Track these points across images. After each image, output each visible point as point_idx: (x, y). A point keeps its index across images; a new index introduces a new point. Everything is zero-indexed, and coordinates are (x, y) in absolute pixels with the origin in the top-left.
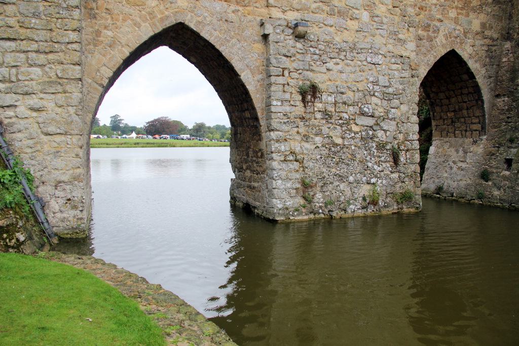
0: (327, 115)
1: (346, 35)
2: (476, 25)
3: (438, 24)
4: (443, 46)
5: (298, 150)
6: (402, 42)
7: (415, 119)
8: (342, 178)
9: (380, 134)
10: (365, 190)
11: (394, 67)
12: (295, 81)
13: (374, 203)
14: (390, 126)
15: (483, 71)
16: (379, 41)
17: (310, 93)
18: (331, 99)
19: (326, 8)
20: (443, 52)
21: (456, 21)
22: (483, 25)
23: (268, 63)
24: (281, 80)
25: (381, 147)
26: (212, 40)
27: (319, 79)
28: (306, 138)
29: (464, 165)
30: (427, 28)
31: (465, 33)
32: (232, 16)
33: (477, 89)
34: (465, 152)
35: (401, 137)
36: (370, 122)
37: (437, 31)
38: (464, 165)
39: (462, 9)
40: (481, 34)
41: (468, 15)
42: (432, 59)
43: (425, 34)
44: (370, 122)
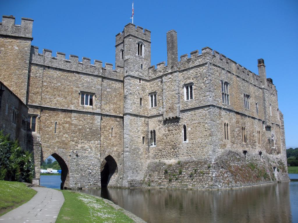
1: (85, 154)
2: (115, 149)
3: (106, 150)
4: (107, 154)
6: (97, 155)
11: (95, 160)
19: (82, 149)
20: (107, 155)
21: (110, 149)
22: (117, 149)
26: (60, 156)
30: (103, 151)
31: (112, 151)
32: (64, 151)
34: (115, 177)
37: (106, 151)
40: (116, 151)
41: (113, 147)
42: (105, 157)
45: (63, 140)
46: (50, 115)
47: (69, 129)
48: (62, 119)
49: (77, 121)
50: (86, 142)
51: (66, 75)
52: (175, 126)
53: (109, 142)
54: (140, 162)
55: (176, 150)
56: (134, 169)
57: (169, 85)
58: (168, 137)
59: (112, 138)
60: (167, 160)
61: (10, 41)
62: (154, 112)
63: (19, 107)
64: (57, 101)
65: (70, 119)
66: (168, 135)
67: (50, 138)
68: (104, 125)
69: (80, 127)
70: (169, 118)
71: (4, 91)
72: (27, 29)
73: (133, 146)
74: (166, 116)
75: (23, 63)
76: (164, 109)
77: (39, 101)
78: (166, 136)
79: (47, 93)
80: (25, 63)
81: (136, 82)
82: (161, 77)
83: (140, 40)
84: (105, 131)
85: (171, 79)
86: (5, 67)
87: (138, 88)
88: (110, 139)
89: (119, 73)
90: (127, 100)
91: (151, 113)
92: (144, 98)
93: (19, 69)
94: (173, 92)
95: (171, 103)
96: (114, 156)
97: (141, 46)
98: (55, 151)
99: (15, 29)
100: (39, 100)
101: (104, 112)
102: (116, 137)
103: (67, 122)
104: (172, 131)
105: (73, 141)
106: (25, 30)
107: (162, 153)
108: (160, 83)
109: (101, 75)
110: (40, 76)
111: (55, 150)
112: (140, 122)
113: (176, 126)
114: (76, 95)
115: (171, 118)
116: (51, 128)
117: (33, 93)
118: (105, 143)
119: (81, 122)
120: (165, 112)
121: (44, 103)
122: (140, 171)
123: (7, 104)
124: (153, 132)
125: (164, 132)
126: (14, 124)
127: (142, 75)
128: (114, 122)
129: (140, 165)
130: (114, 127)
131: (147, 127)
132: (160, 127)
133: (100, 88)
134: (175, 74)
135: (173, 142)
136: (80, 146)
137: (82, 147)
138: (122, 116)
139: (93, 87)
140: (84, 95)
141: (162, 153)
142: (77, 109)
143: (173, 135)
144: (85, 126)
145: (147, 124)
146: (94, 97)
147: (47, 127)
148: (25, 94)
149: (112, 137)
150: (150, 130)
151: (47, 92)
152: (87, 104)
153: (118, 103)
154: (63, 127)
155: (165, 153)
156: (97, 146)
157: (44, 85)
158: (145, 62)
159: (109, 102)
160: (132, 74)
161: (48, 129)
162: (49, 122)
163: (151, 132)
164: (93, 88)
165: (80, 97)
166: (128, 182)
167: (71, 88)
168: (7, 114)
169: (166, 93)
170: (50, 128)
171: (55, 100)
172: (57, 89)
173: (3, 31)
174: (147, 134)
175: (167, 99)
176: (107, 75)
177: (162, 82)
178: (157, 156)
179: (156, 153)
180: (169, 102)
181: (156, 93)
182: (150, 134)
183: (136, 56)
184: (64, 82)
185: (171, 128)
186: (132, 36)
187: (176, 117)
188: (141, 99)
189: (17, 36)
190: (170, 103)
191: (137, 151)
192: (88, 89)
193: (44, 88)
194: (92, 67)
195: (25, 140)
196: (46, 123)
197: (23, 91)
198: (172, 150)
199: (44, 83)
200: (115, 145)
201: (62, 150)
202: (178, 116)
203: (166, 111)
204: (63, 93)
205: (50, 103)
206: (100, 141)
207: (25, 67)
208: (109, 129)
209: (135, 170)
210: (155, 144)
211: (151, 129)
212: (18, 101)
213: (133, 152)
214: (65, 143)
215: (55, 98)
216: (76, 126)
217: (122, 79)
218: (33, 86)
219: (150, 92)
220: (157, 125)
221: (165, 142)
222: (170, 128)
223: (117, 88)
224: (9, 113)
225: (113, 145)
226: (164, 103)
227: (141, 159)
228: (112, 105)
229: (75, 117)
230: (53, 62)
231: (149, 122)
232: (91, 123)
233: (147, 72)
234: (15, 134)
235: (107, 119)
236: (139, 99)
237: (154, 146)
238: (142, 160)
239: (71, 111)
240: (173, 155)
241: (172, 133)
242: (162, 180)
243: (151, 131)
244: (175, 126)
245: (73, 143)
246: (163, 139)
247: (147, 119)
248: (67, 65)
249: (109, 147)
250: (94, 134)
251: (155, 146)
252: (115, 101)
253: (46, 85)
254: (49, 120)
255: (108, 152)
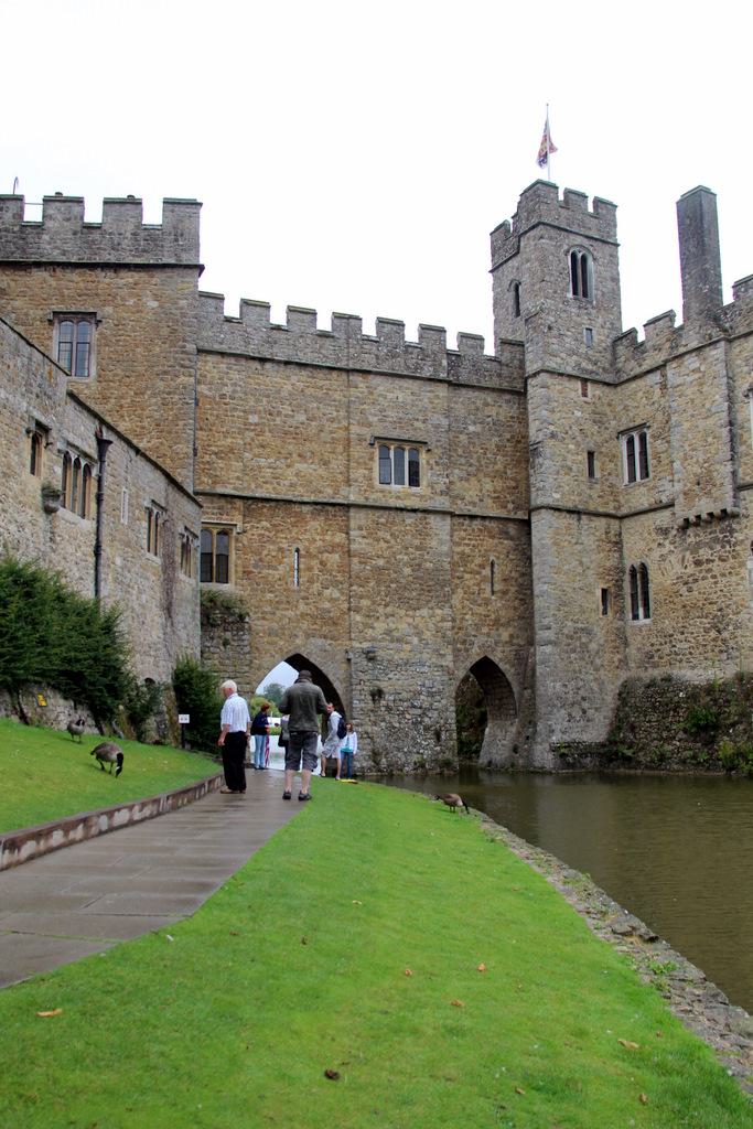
0: (389, 709)
2: (505, 636)
4: (478, 654)
5: (370, 731)
6: (443, 656)
7: (453, 708)
8: (399, 749)
9: (426, 719)
10: (416, 758)
12: (368, 688)
13: (423, 766)
14: (436, 714)
15: (513, 670)
16: (425, 656)
17: (377, 694)
18: (392, 698)
20: (478, 658)
21: (488, 635)
22: (511, 636)
23: (351, 677)
24: (359, 687)
25: (427, 729)
26: (316, 663)
27: (383, 685)
28: (375, 724)
29: (505, 742)
30: (464, 642)
31: (496, 643)
33: (509, 684)
35: (442, 721)
36: (419, 712)
38: (505, 742)
39: (493, 625)
40: (510, 643)
41: (498, 630)
43: (463, 647)
44: (419, 712)
45: (324, 609)
46: (274, 525)
47: (345, 568)
48: (318, 538)
49: (367, 541)
50: (402, 612)
51: (321, 383)
52: (718, 547)
53: (481, 610)
54: (596, 679)
55: (725, 635)
56: (573, 705)
57: (692, 397)
58: (694, 586)
59: (493, 598)
60: (696, 671)
61: (131, 280)
62: (641, 497)
63: (166, 498)
64: (297, 475)
65: (344, 535)
66: (696, 580)
67: (277, 602)
68: (463, 553)
69: (381, 562)
70: (698, 517)
71: (111, 442)
72: (182, 235)
73: (570, 624)
74: (683, 511)
75: (177, 353)
76: (678, 487)
77: (238, 478)
78: (686, 583)
79: (261, 450)
80: (183, 352)
81: (573, 394)
82: (661, 367)
83: (579, 240)
84: (468, 573)
85: (701, 375)
86: (119, 372)
87: (578, 414)
88: (487, 602)
89: (507, 365)
90: (541, 460)
91: (627, 501)
92: (603, 450)
93: (165, 373)
94: (710, 422)
95: (701, 460)
96: (501, 660)
97: (584, 259)
98: (298, 647)
99: (145, 240)
100: (237, 474)
101: (460, 508)
102: (505, 593)
103: (333, 548)
104: (710, 566)
105: (358, 610)
106: (176, 240)
107: (674, 646)
108: (658, 392)
109: (443, 375)
110: (234, 391)
111: (298, 641)
112: (592, 537)
113: (723, 547)
114: (358, 451)
115: (704, 516)
116: (280, 568)
117: (216, 453)
118: (467, 617)
119: (385, 545)
120: (682, 497)
121: (253, 486)
122: (596, 709)
123: (124, 489)
124: (638, 569)
125: (679, 569)
126: (151, 555)
127: (590, 367)
128: (496, 541)
129: (596, 689)
130: (498, 558)
131: (617, 555)
132: (665, 551)
133: (445, 422)
134: (714, 352)
135: (716, 603)
136: (380, 626)
137: (388, 632)
138: (526, 518)
139: (417, 420)
140: (389, 449)
141: (674, 646)
142: (367, 499)
143: (714, 577)
144: (398, 557)
145: (618, 544)
146: (423, 458)
147: (269, 567)
148: (188, 457)
149: (493, 592)
150: (628, 564)
151: (262, 446)
152: (400, 481)
153: (509, 472)
154: (321, 563)
155: (686, 646)
156: (440, 625)
157: (251, 424)
158: (600, 320)
159: (478, 470)
160: (552, 364)
161: (270, 571)
162: (272, 547)
163: (633, 571)
164: (416, 424)
165: (377, 458)
166: (554, 749)
167: (341, 428)
168: (125, 521)
169: (683, 426)
170: (277, 570)
171: (289, 471)
172: (296, 434)
173: (105, 250)
174: (617, 581)
175: (687, 448)
176: (463, 379)
177: (664, 386)
178: (656, 659)
179: (652, 645)
180: (695, 459)
181: (645, 430)
182: (627, 578)
183: (566, 302)
184: (318, 408)
185: (704, 553)
186: (544, 224)
187: (724, 511)
188: (591, 454)
189: (152, 262)
190: (697, 461)
191: (584, 640)
192: (402, 428)
193: (252, 434)
194: (410, 350)
195: (194, 612)
196: (265, 552)
197: (181, 446)
198: (713, 634)
199: (250, 417)
200: (503, 620)
201: (320, 642)
202: (729, 510)
203: (685, 494)
204: (316, 446)
205: (272, 483)
206: (451, 607)
207: (182, 366)
208: (480, 566)
209: (577, 707)
210: (647, 616)
211: (631, 560)
212: (163, 478)
213: (569, 645)
214: (331, 618)
215: (288, 466)
216: (365, 558)
217: (519, 386)
218: (214, 428)
219: (622, 429)
220: (654, 546)
221: (684, 607)
222: (701, 552)
223: (501, 418)
224: (134, 519)
225: (497, 623)
226: (677, 465)
227: (597, 670)
228: (488, 480)
229: (360, 528)
230: (275, 343)
231: (625, 537)
232: (417, 548)
233: (608, 356)
234: (157, 589)
235: (473, 530)
236: (586, 455)
237: (642, 621)
238: (602, 672)
239: (348, 506)
240: (717, 650)
241: (709, 570)
242: (678, 744)
243: (632, 566)
244: (718, 547)
245: (358, 618)
246: (678, 594)
247: (615, 524)
248: (323, 351)
249: (485, 630)
250: (431, 583)
251: (647, 621)
252: (499, 466)
253: (256, 425)
254: (273, 543)
255: (479, 647)
